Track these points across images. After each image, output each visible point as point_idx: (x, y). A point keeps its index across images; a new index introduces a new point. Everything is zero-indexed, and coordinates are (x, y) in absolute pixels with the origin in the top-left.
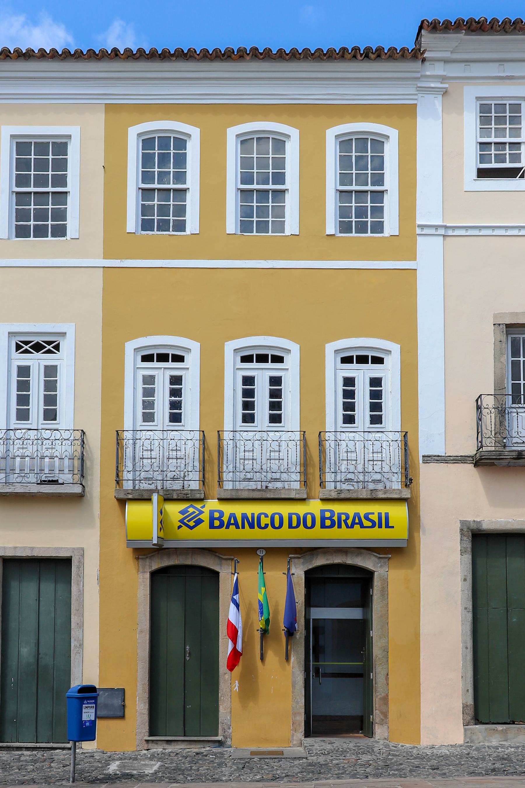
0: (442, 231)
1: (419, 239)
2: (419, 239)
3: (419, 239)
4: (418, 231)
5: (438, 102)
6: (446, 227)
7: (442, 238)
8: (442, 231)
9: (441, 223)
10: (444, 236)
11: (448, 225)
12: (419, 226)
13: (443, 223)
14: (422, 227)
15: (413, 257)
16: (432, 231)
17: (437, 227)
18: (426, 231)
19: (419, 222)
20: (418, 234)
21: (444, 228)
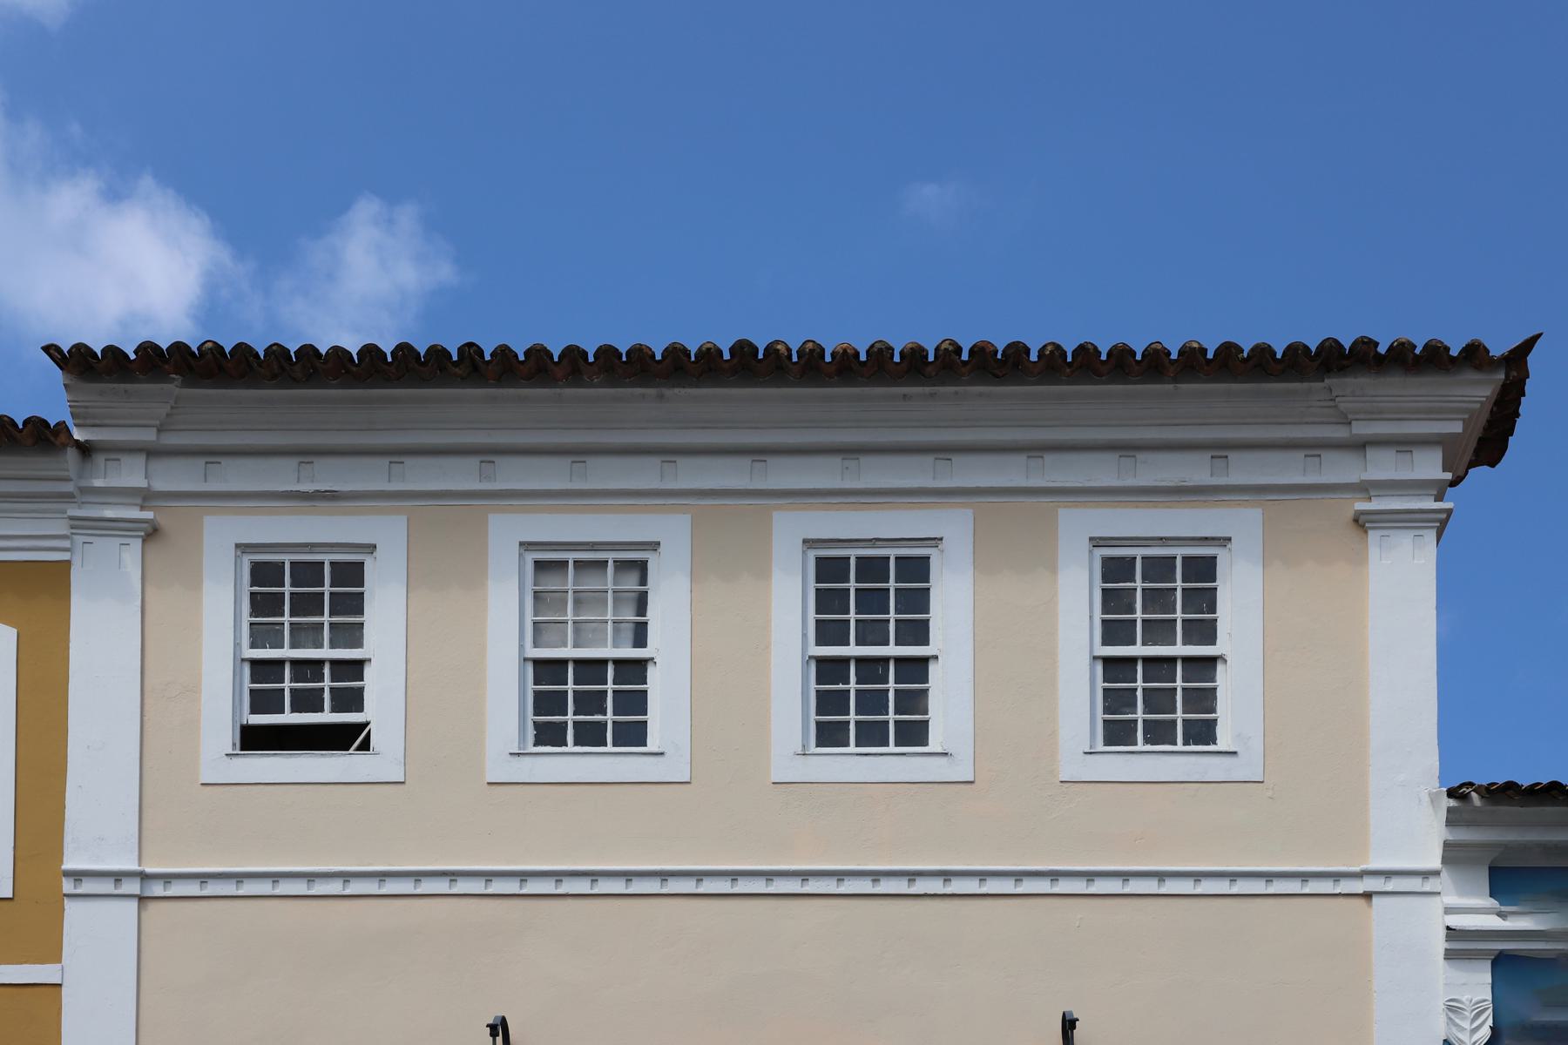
0: (133, 887)
1: (69, 905)
2: (72, 909)
3: (69, 905)
4: (68, 886)
5: (131, 553)
6: (144, 877)
7: (134, 904)
8: (133, 887)
9: (133, 866)
10: (142, 899)
11: (149, 870)
12: (68, 874)
13: (140, 866)
14: (79, 876)
15: (53, 953)
16: (107, 887)
17: (118, 876)
18: (88, 887)
19: (69, 864)
20: (65, 895)
21: (138, 880)
